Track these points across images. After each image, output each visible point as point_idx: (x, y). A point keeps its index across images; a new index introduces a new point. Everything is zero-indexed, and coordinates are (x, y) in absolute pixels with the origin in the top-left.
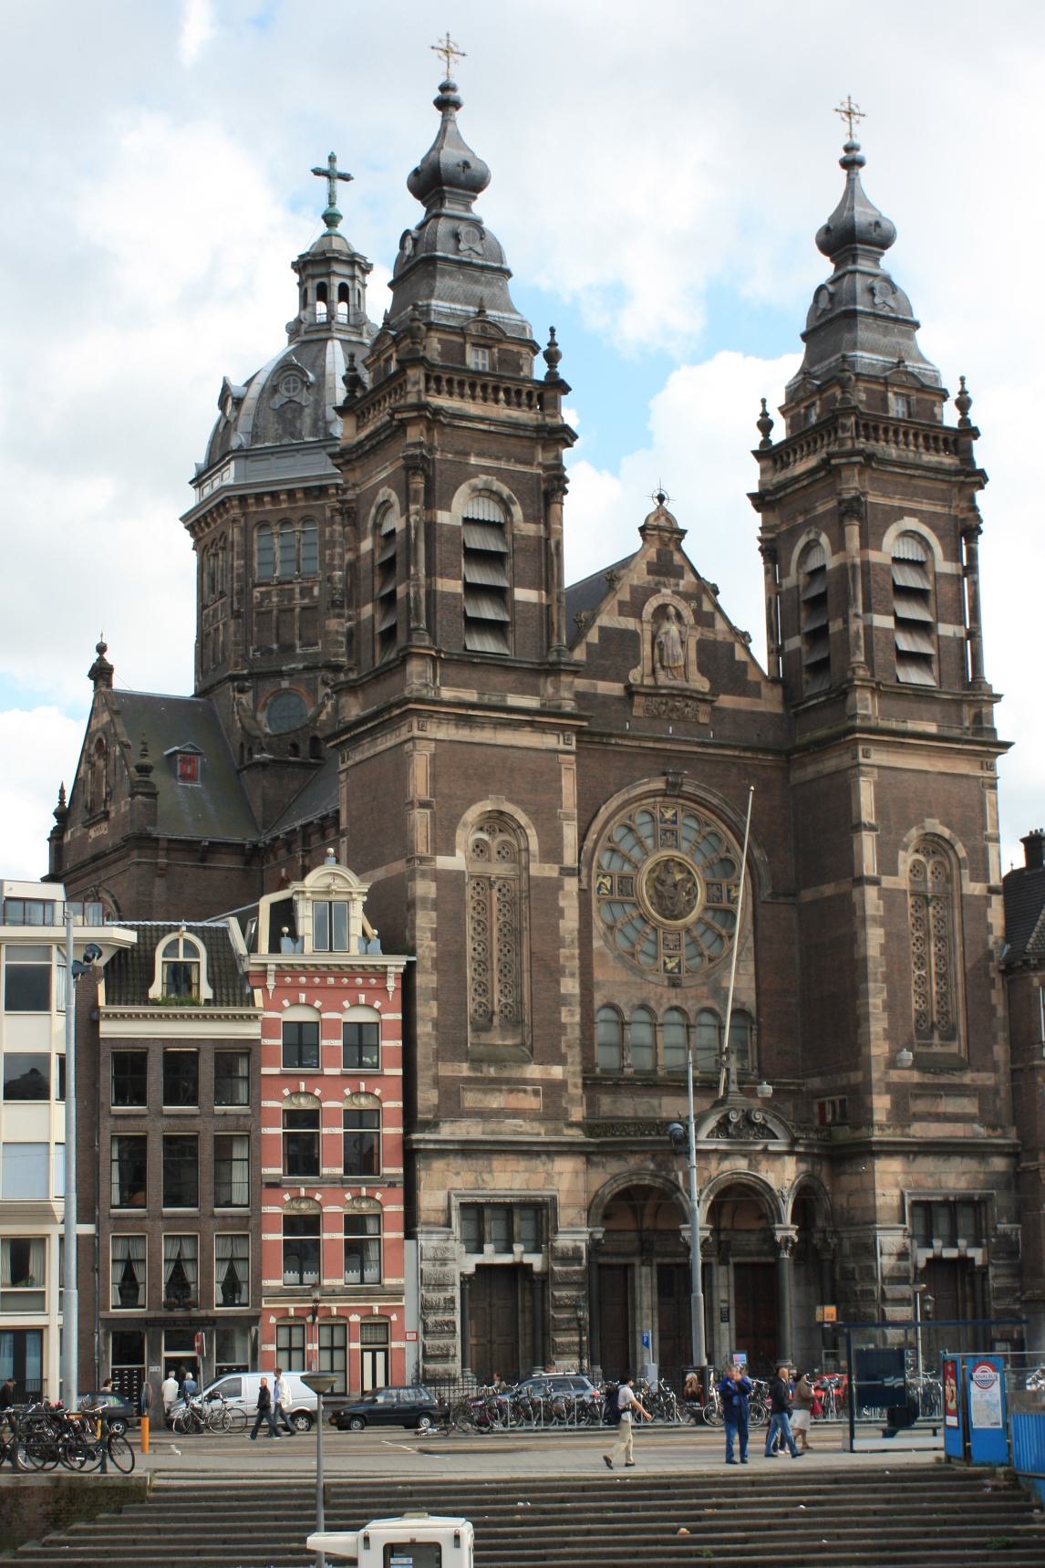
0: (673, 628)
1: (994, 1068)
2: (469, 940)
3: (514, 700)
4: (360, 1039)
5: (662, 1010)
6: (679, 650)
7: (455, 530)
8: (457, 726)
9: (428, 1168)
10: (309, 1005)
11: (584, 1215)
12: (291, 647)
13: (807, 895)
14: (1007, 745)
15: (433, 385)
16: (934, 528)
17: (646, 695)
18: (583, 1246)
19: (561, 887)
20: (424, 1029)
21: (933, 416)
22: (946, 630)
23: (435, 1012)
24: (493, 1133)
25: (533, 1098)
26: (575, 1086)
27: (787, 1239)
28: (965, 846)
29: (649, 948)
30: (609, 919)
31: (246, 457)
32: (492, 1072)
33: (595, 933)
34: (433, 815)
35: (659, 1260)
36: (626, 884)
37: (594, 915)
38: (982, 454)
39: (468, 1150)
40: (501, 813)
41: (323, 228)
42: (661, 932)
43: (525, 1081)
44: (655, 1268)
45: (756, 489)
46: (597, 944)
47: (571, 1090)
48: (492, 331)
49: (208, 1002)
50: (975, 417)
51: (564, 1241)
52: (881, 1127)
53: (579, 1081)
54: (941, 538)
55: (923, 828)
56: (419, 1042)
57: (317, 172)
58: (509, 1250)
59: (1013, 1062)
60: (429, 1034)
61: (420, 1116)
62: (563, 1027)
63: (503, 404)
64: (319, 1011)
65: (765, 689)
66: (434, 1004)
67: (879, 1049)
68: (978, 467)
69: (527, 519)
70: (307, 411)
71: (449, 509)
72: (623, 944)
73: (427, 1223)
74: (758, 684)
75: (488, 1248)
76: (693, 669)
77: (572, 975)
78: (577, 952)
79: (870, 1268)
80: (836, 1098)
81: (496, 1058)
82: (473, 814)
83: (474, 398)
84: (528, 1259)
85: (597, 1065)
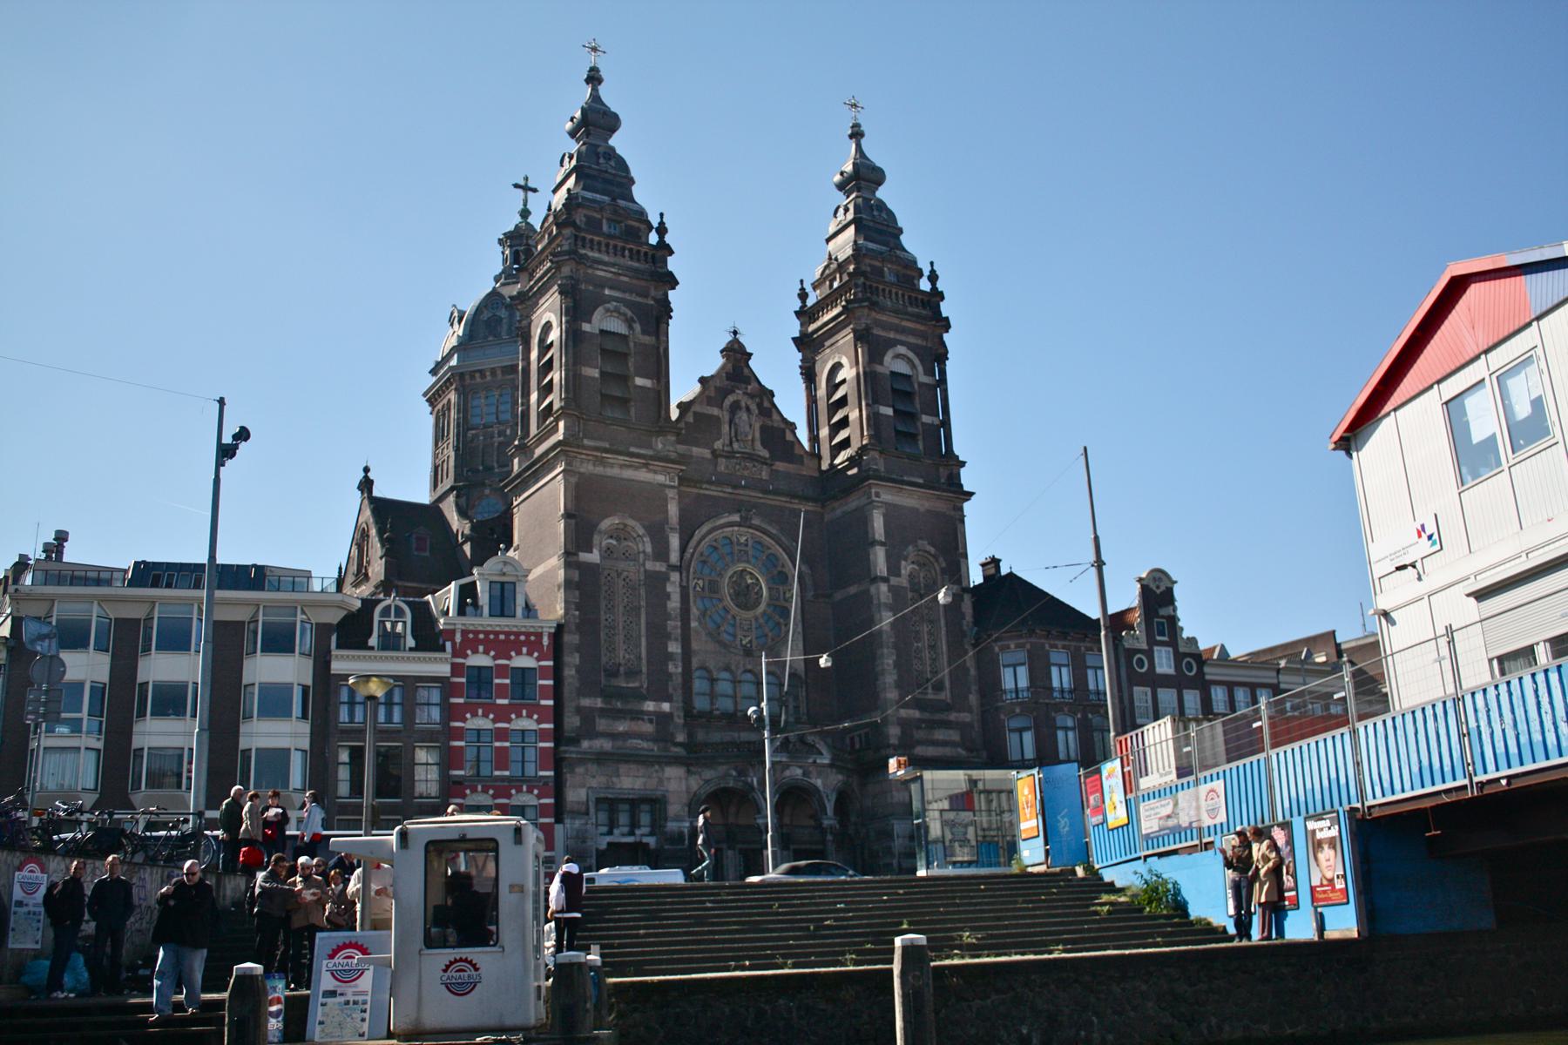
0: (744, 416)
1: (970, 711)
2: (602, 613)
3: (632, 449)
4: (523, 677)
5: (740, 671)
6: (747, 428)
7: (592, 334)
8: (594, 465)
9: (572, 772)
10: (486, 652)
11: (686, 809)
12: (492, 468)
13: (838, 596)
14: (971, 494)
15: (580, 243)
16: (917, 354)
17: (726, 457)
18: (686, 831)
19: (668, 579)
20: (569, 672)
21: (914, 285)
22: (926, 419)
23: (577, 661)
24: (618, 748)
25: (649, 725)
26: (679, 717)
27: (831, 827)
28: (945, 560)
29: (731, 630)
30: (701, 607)
31: (465, 349)
32: (619, 705)
33: (692, 617)
34: (576, 524)
35: (739, 846)
36: (713, 587)
37: (692, 604)
38: (946, 309)
39: (601, 758)
40: (625, 525)
41: (518, 219)
42: (738, 618)
43: (643, 712)
44: (737, 852)
45: (797, 335)
46: (694, 624)
47: (677, 720)
48: (621, 211)
49: (411, 649)
50: (940, 286)
51: (672, 826)
52: (893, 746)
53: (682, 714)
54: (921, 361)
55: (916, 546)
56: (566, 683)
57: (516, 186)
58: (632, 833)
59: (982, 705)
60: (572, 676)
61: (566, 734)
62: (670, 675)
63: (627, 258)
64: (495, 658)
65: (806, 460)
66: (577, 655)
67: (892, 695)
68: (944, 315)
70: (505, 321)
71: (590, 322)
72: (711, 625)
73: (572, 812)
74: (802, 456)
75: (616, 831)
76: (758, 445)
77: (676, 640)
78: (679, 624)
79: (890, 848)
80: (862, 732)
81: (622, 694)
82: (605, 524)
83: (608, 253)
84: (645, 840)
85: (694, 708)
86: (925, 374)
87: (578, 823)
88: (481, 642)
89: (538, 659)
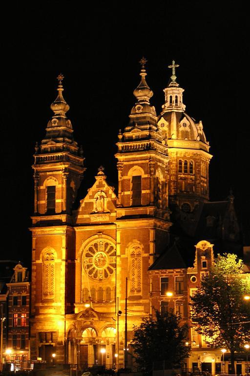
16: (142, 167)
20: (33, 296)
69: (59, 184)
84: (52, 344)
86: (145, 174)
87: (34, 339)
88: (15, 290)
89: (27, 293)
